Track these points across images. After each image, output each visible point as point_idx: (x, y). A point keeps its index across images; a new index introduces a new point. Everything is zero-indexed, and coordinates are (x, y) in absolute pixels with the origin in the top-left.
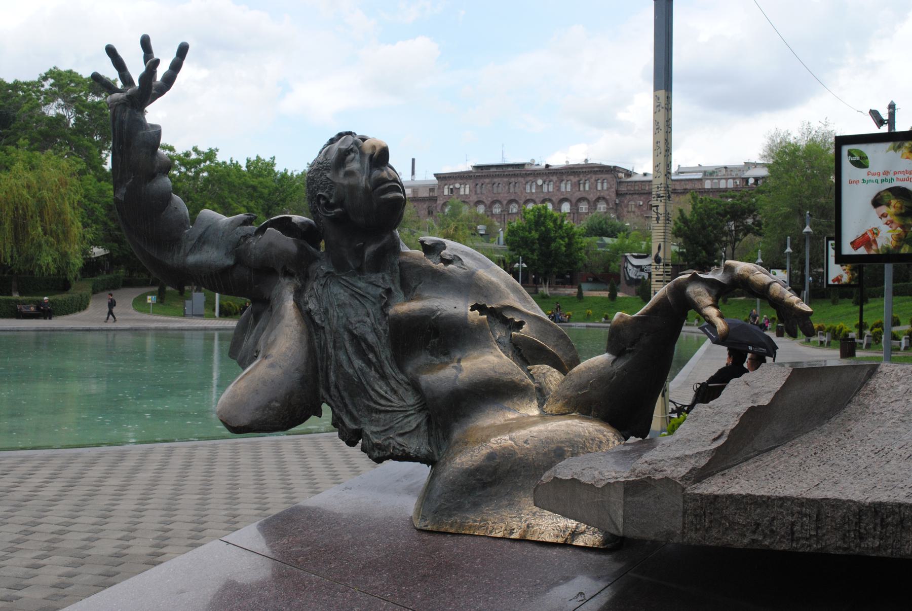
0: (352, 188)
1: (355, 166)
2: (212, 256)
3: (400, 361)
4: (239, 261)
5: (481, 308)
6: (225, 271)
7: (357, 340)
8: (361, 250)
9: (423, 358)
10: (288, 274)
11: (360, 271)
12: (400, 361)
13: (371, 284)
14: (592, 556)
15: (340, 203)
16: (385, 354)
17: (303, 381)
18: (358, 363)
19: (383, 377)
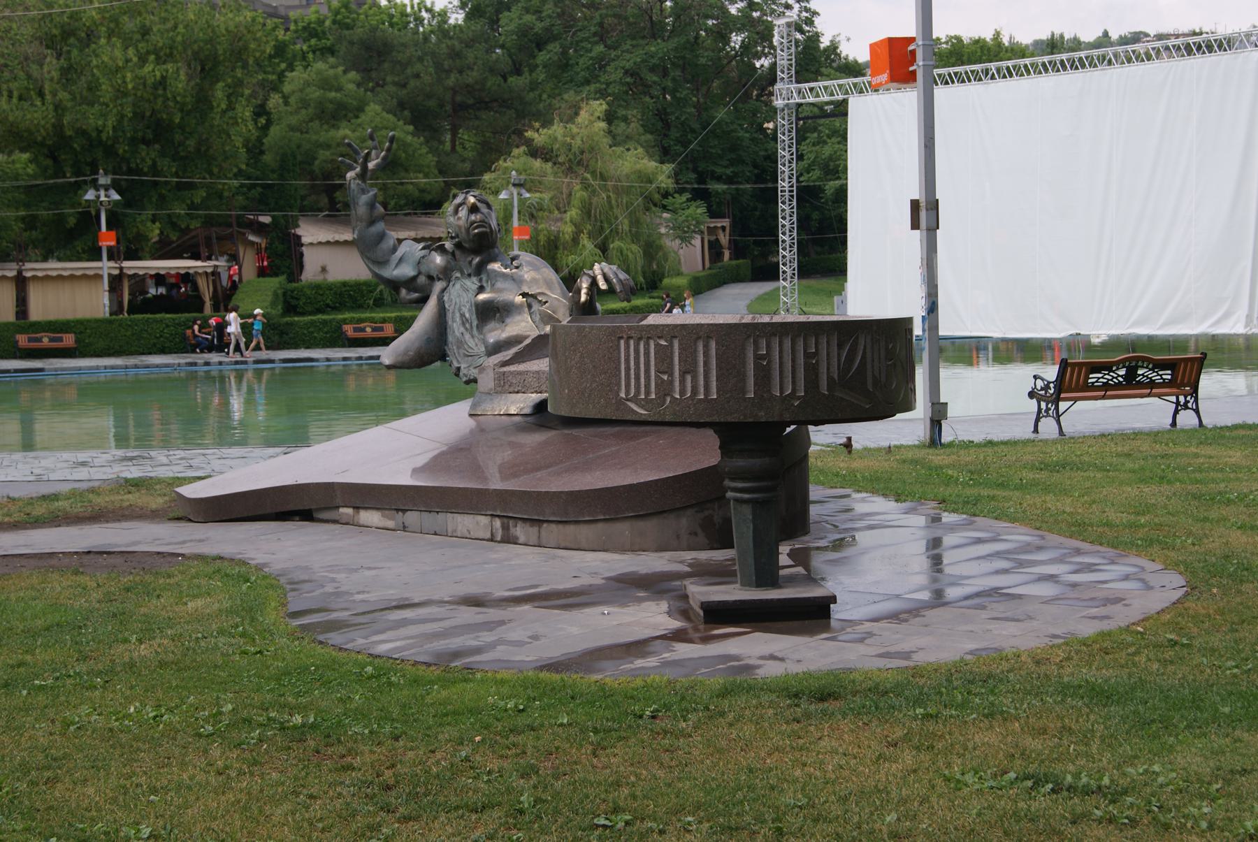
0: (460, 227)
1: (463, 213)
2: (407, 271)
3: (480, 328)
4: (420, 273)
5: (524, 295)
6: (414, 278)
7: (462, 315)
8: (470, 262)
9: (492, 325)
10: (439, 279)
11: (469, 275)
12: (480, 328)
13: (472, 283)
14: (528, 419)
15: (457, 236)
16: (475, 323)
17: (429, 340)
18: (462, 329)
19: (473, 337)
